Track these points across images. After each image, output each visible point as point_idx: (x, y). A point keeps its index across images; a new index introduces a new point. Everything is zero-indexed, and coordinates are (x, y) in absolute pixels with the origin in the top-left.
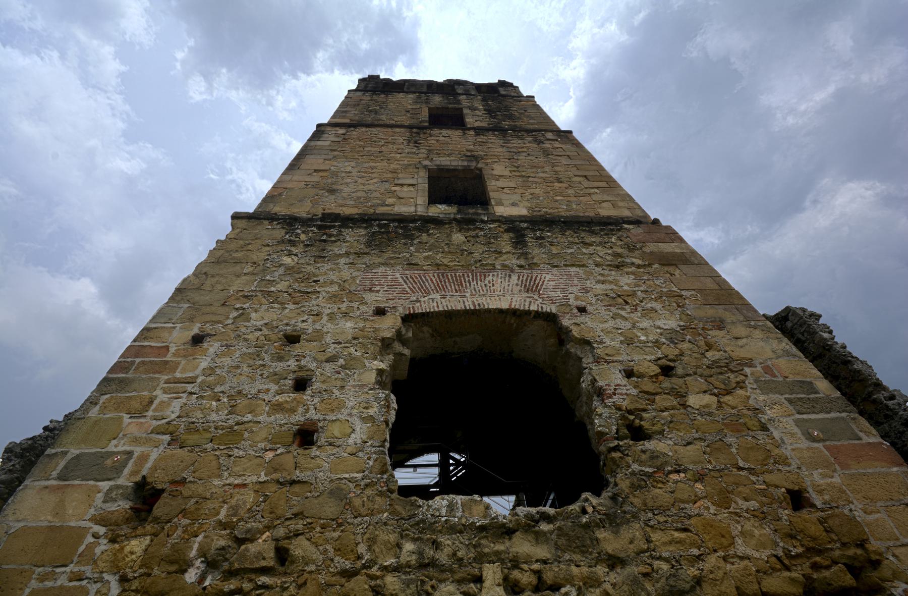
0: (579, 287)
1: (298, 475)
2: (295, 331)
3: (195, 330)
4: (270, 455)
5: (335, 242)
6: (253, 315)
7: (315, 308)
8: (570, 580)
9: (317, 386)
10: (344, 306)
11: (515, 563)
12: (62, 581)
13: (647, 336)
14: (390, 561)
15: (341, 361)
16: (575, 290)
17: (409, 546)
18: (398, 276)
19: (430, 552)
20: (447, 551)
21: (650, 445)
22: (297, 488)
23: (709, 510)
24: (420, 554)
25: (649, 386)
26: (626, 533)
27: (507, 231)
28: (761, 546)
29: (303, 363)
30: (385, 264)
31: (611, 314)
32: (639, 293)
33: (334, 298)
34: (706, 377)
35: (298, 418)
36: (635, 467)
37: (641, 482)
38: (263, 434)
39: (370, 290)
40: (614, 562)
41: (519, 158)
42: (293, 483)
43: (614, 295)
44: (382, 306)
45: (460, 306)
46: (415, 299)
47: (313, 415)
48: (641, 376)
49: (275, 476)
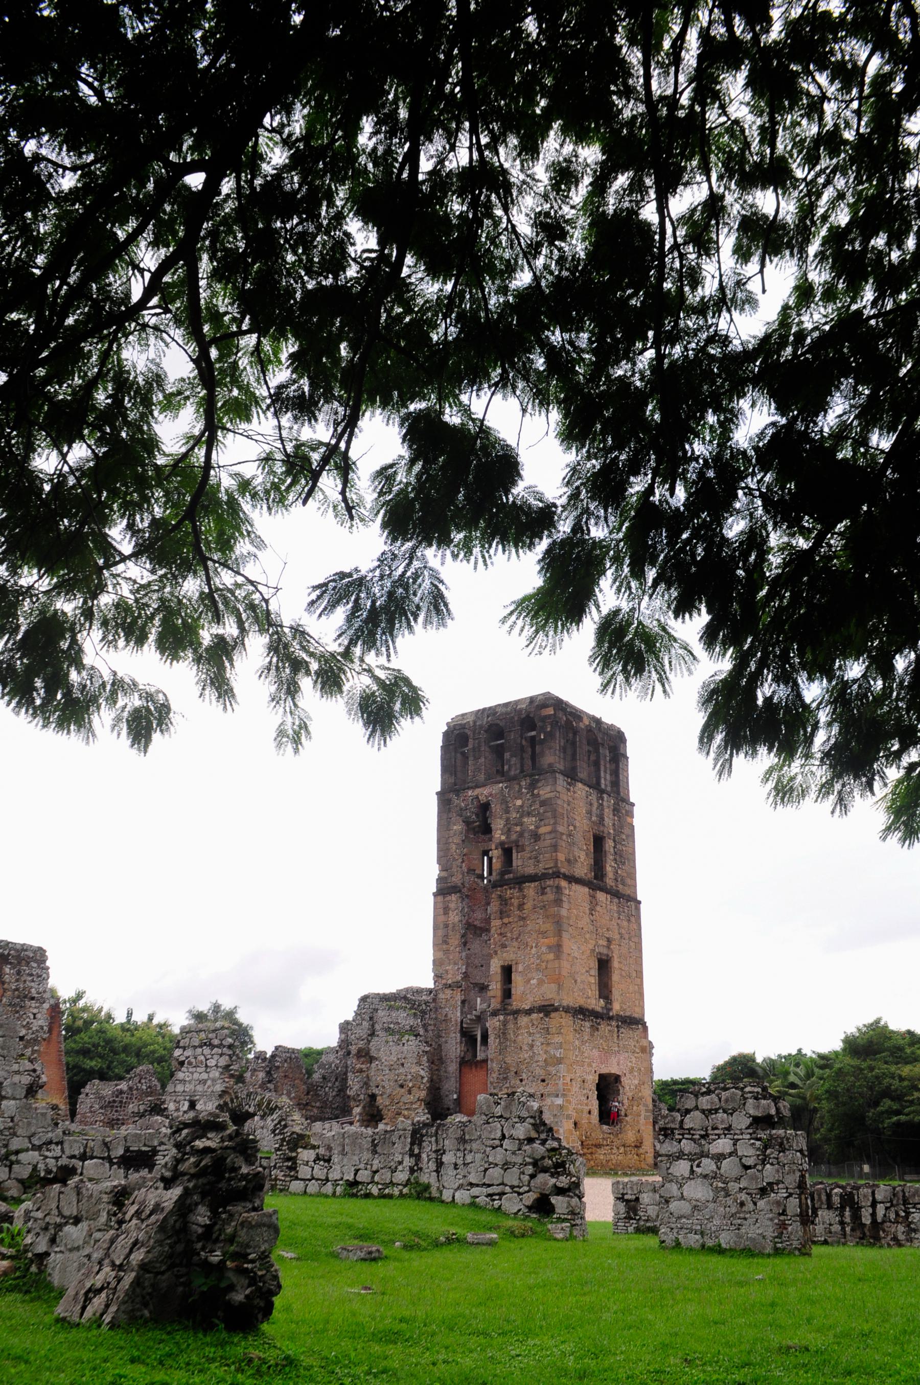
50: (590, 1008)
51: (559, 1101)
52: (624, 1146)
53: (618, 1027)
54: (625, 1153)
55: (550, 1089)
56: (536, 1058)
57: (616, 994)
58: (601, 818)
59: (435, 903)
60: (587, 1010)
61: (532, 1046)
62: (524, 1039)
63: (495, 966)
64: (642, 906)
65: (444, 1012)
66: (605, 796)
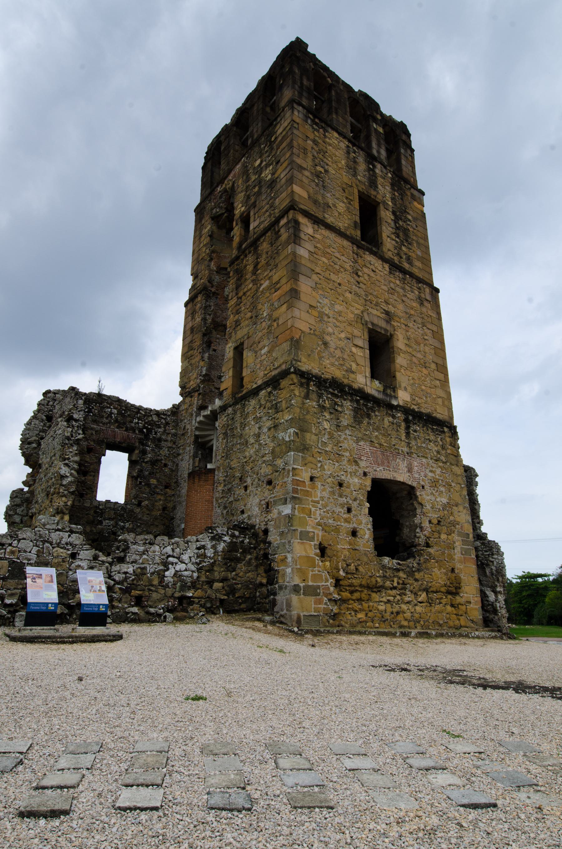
1: (357, 548)
2: (341, 480)
3: (309, 474)
5: (341, 412)
6: (325, 467)
8: (409, 584)
9: (353, 512)
12: (317, 572)
15: (358, 502)
16: (422, 474)
18: (368, 450)
19: (385, 574)
20: (388, 574)
21: (430, 550)
22: (356, 551)
23: (436, 570)
24: (383, 573)
25: (434, 529)
28: (443, 581)
32: (440, 481)
34: (447, 527)
35: (351, 526)
36: (426, 557)
37: (426, 561)
38: (344, 531)
40: (416, 580)
42: (356, 550)
44: (366, 470)
46: (375, 468)
48: (432, 524)
49: (351, 547)
50: (355, 386)
51: (287, 510)
52: (426, 590)
53: (406, 421)
54: (430, 602)
55: (278, 492)
56: (262, 452)
57: (402, 378)
58: (373, 183)
59: (186, 313)
60: (350, 387)
61: (258, 436)
62: (252, 429)
63: (229, 350)
64: (440, 295)
65: (182, 425)
66: (379, 166)
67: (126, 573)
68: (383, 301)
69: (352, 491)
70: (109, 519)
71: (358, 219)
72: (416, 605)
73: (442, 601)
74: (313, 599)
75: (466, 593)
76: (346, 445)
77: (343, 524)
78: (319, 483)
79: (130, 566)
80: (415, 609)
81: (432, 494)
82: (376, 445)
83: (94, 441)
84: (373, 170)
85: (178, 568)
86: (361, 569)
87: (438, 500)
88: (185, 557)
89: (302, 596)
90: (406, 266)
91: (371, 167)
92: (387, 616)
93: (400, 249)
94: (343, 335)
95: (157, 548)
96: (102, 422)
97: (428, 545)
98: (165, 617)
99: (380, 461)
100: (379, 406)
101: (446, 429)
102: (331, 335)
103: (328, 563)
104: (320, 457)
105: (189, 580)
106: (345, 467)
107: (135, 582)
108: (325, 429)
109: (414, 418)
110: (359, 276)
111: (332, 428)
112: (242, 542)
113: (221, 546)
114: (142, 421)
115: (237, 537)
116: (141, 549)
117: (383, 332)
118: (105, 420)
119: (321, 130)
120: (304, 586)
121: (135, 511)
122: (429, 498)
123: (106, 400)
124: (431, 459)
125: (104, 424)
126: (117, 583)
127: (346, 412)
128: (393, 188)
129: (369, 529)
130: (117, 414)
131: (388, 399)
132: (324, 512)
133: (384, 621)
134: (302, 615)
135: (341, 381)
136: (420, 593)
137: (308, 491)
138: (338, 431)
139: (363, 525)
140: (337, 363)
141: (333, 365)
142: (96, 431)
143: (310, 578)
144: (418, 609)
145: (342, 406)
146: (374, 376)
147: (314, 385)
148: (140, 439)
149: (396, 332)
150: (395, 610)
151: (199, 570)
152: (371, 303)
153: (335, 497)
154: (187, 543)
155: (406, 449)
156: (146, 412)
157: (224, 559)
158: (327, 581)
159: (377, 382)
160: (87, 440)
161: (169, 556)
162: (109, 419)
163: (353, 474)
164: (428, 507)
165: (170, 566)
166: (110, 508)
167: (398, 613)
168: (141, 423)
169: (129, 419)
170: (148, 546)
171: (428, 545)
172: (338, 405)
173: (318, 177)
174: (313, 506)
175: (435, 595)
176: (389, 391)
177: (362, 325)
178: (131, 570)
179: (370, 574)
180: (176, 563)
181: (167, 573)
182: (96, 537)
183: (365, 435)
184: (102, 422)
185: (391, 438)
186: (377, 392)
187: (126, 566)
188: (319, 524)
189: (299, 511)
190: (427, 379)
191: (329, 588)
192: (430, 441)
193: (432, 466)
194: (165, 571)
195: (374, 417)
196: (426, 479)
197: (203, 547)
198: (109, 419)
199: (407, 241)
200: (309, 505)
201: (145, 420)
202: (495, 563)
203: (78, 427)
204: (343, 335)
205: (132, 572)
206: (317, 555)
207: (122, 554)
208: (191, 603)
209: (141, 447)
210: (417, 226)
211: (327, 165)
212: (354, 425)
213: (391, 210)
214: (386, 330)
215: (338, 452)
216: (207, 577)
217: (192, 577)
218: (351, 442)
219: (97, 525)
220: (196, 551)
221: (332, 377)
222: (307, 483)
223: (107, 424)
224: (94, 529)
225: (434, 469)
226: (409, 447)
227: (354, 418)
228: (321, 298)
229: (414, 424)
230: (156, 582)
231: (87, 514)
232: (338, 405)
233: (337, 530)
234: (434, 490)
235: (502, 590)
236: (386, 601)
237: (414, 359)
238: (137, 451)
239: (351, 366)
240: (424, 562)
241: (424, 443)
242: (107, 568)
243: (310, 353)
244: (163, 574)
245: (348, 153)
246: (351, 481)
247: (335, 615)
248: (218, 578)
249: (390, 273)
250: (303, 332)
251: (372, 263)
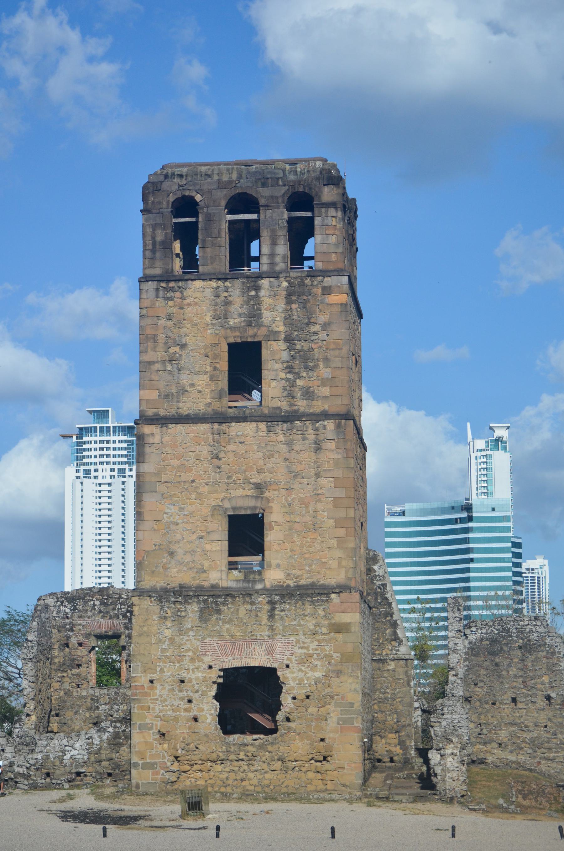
0: (290, 652)
1: (196, 730)
3: (149, 678)
4: (187, 725)
7: (186, 666)
9: (194, 702)
10: (196, 664)
11: (248, 752)
12: (154, 753)
13: (308, 681)
14: (220, 750)
15: (200, 693)
16: (288, 653)
17: (224, 748)
18: (215, 645)
19: (229, 749)
21: (289, 724)
23: (298, 743)
24: (227, 749)
26: (274, 747)
27: (268, 603)
29: (188, 693)
30: (209, 636)
31: (298, 668)
32: (315, 656)
33: (192, 660)
35: (192, 714)
36: (283, 731)
39: (206, 655)
40: (269, 752)
41: (294, 487)
43: (303, 657)
44: (211, 664)
45: (240, 665)
46: (222, 660)
47: (196, 713)
49: (191, 730)
50: (206, 584)
66: (265, 282)
67: (36, 759)
68: (255, 472)
69: (193, 686)
70: (106, 704)
71: (224, 384)
72: (265, 773)
73: (302, 769)
74: (151, 771)
75: (339, 760)
76: (189, 646)
77: (182, 714)
78: (159, 684)
79: (38, 754)
80: (264, 777)
81: (300, 670)
82: (227, 637)
83: (82, 635)
84: (257, 296)
85: (72, 753)
86: (200, 747)
87: (307, 675)
88: (77, 746)
89: (140, 770)
90: (302, 405)
91: (253, 293)
92: (230, 782)
93: (293, 385)
94: (194, 537)
95: (56, 741)
96: (87, 616)
97: (288, 720)
98: (63, 785)
99: (228, 651)
100: (233, 597)
101: (333, 596)
102: (179, 542)
103: (166, 746)
104: (160, 662)
105: (81, 761)
106: (186, 666)
107: (43, 764)
108: (166, 637)
109: (283, 596)
110: (220, 459)
111: (174, 634)
112: (124, 731)
113: (105, 736)
114: (125, 605)
115: (120, 727)
116: (45, 743)
117: (249, 512)
118: (89, 614)
119: (178, 294)
120: (142, 764)
121: (127, 694)
122: (295, 675)
123: (88, 593)
124: (304, 634)
125: (89, 617)
126: (33, 765)
127: (190, 615)
128: (289, 301)
129: (211, 714)
130: (100, 605)
131: (250, 585)
132: (163, 706)
133: (226, 787)
134: (140, 782)
135: (189, 585)
136: (274, 763)
137: (146, 692)
138: (181, 635)
139: (205, 712)
140: (185, 569)
141: (179, 571)
142: (83, 626)
143: (148, 757)
144: (267, 776)
145: (186, 611)
146: (232, 566)
147: (155, 600)
148: (125, 624)
149: (270, 504)
150: (238, 778)
151: (89, 753)
152: (235, 484)
153: (175, 693)
154: (79, 736)
155: (267, 633)
156: (127, 596)
157: (109, 744)
158: (164, 757)
159: (235, 572)
160: (76, 636)
161: (65, 746)
162: (93, 611)
163: (196, 670)
164: (292, 684)
165: (67, 753)
166: (104, 694)
167: (242, 780)
168: (124, 608)
169: (111, 607)
170: (49, 741)
171: (288, 720)
172: (181, 611)
173: (171, 360)
174: (152, 703)
175: (294, 763)
176: (252, 576)
177: (220, 517)
178: (39, 757)
179: (210, 750)
180: (71, 750)
181: (65, 757)
182: (95, 721)
183: (212, 631)
184: (87, 616)
185: (247, 626)
186: (235, 582)
187: (36, 754)
188: (156, 717)
189: (138, 709)
190: (315, 544)
191: (166, 764)
192: (304, 615)
193: (304, 643)
194: (63, 756)
195: (226, 611)
196: (293, 657)
197: (91, 738)
198: (93, 611)
199: (306, 367)
200: (148, 702)
201: (127, 604)
202: (444, 723)
203: (32, 647)
204: (194, 537)
205: (40, 758)
206: (155, 740)
207: (34, 748)
208: (86, 776)
209: (127, 631)
210: (328, 335)
211: (186, 335)
212: (199, 625)
213: (283, 336)
214: (255, 508)
215: (180, 654)
216: (95, 758)
217: (83, 759)
218: (194, 642)
219: (95, 710)
220: (86, 741)
221: (180, 584)
222: (146, 687)
223: (92, 616)
224: (92, 714)
225: (306, 645)
226: (272, 630)
227: (200, 617)
228: (168, 508)
229: (281, 604)
230: (57, 763)
231: (85, 702)
232: (181, 611)
233: (176, 719)
234: (304, 666)
235: (456, 751)
236: (229, 770)
237: (297, 526)
238: (123, 637)
239: (203, 566)
240: (281, 736)
241: (295, 620)
242: (25, 757)
243: (154, 569)
244: (61, 758)
245: (217, 296)
246: (193, 676)
247: (172, 782)
248: (104, 758)
249: (269, 431)
250: (147, 552)
251: (240, 433)
